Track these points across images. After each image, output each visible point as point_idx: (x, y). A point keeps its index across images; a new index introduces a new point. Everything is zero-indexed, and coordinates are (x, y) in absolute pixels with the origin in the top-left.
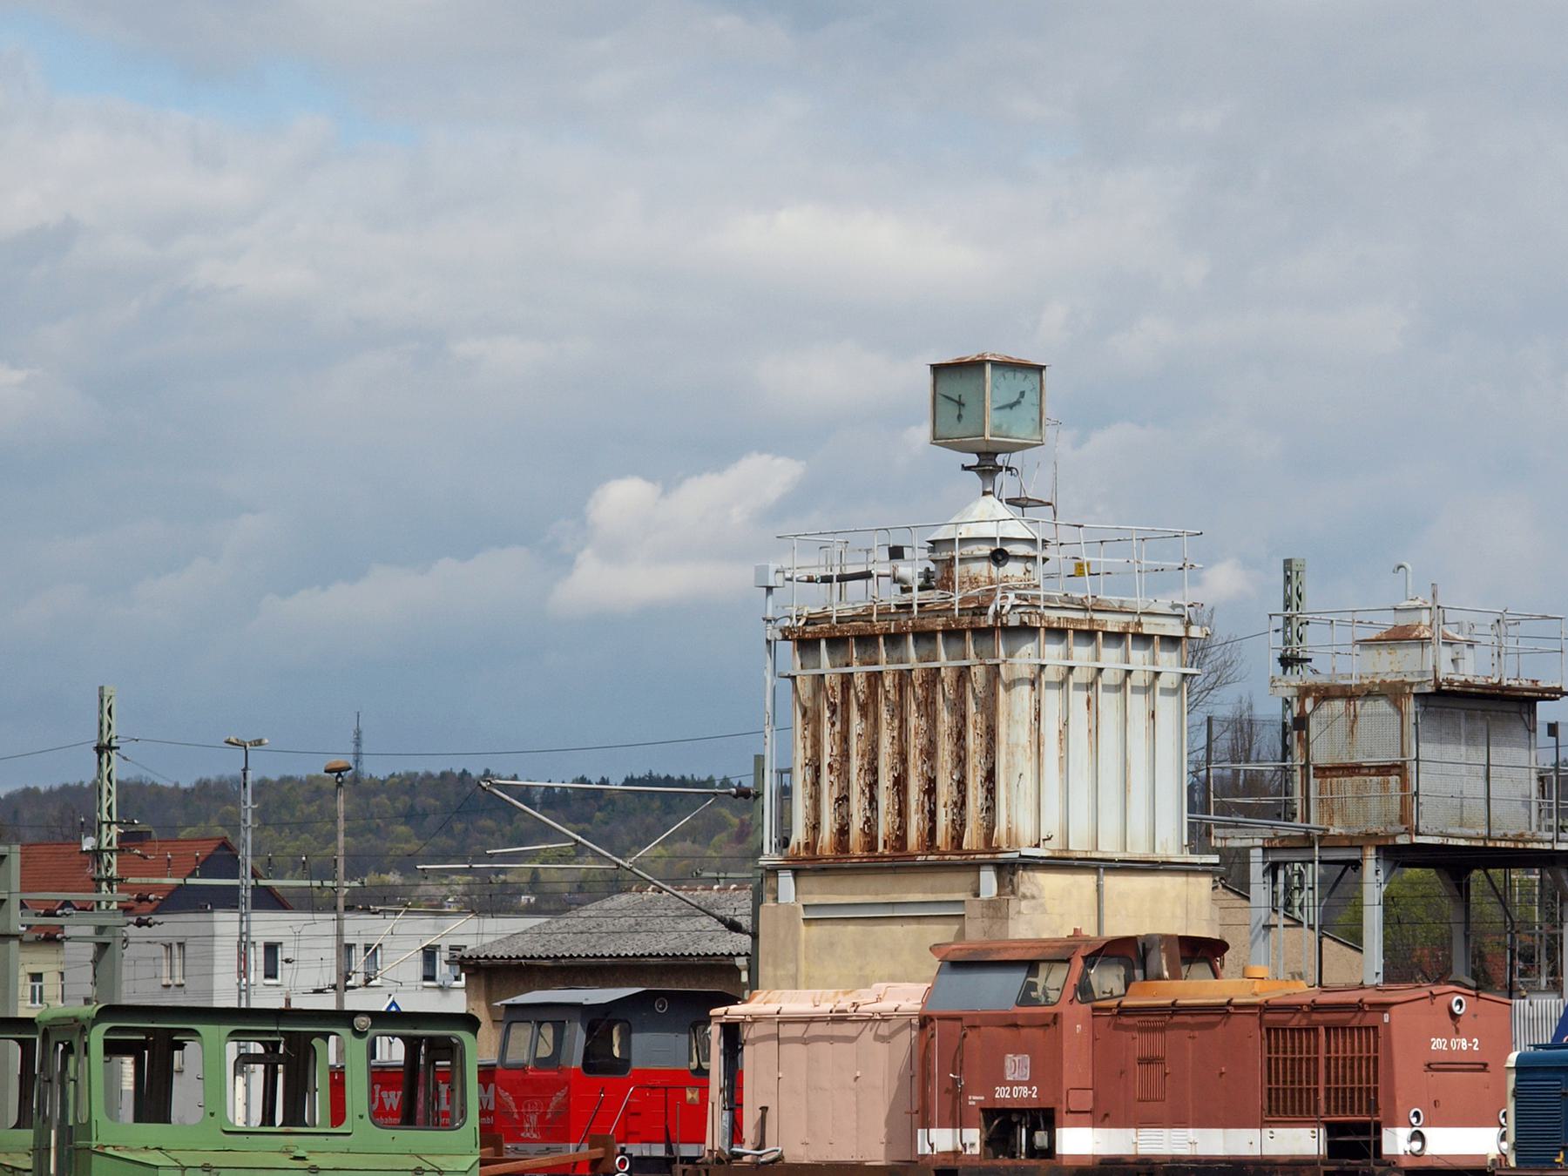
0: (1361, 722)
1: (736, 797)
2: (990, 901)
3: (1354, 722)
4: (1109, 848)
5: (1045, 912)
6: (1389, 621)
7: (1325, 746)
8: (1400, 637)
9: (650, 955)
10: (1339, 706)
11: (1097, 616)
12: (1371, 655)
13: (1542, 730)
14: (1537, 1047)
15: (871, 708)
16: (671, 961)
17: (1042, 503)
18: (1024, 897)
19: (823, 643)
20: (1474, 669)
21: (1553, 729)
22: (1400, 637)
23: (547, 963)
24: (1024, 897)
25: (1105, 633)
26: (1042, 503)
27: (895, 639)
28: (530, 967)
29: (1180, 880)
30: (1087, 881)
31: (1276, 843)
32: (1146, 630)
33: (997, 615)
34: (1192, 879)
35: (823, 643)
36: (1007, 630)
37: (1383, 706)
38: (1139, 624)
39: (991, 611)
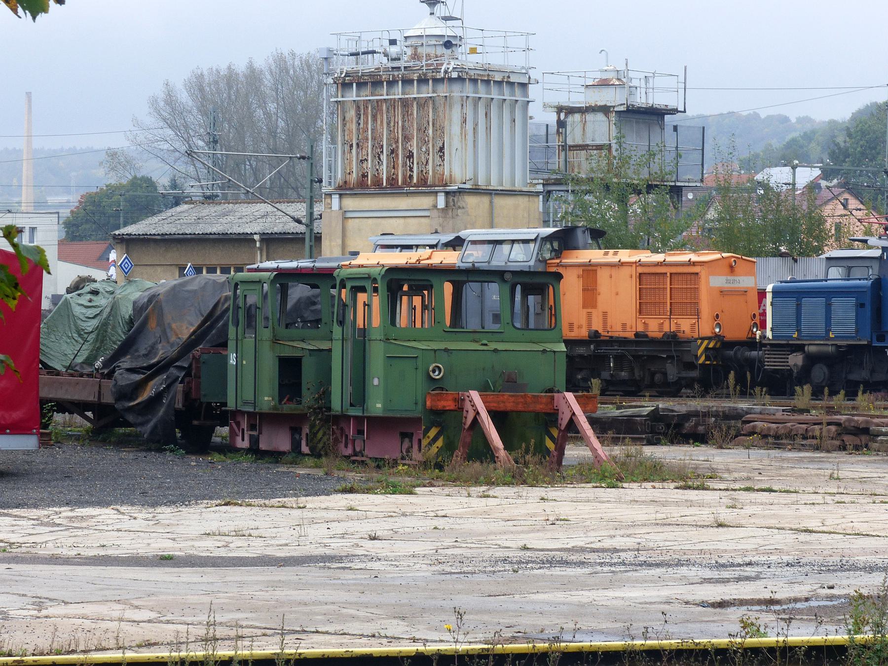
0: (588, 124)
1: (299, 159)
2: (443, 209)
3: (584, 125)
4: (494, 185)
5: (468, 215)
6: (599, 76)
7: (574, 136)
8: (604, 84)
9: (211, 234)
10: (577, 117)
11: (491, 73)
12: (590, 91)
13: (669, 130)
14: (781, 282)
15: (379, 116)
16: (221, 237)
17: (457, 19)
18: (459, 207)
19: (354, 85)
20: (640, 100)
21: (675, 128)
22: (604, 84)
23: (159, 237)
24: (459, 207)
25: (494, 81)
26: (457, 19)
27: (391, 83)
28: (149, 240)
29: (526, 199)
30: (485, 200)
31: (550, 182)
32: (512, 80)
33: (446, 72)
34: (531, 198)
35: (354, 85)
36: (451, 79)
37: (600, 117)
38: (509, 77)
39: (442, 71)
